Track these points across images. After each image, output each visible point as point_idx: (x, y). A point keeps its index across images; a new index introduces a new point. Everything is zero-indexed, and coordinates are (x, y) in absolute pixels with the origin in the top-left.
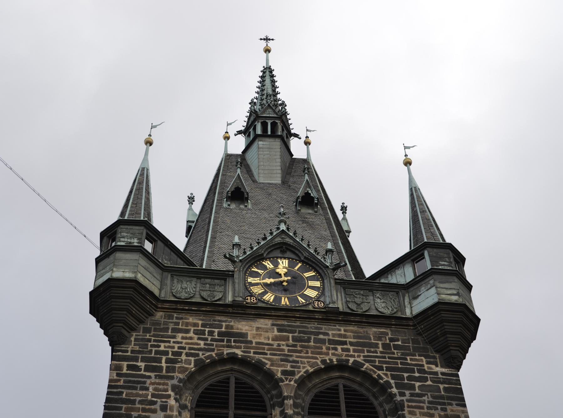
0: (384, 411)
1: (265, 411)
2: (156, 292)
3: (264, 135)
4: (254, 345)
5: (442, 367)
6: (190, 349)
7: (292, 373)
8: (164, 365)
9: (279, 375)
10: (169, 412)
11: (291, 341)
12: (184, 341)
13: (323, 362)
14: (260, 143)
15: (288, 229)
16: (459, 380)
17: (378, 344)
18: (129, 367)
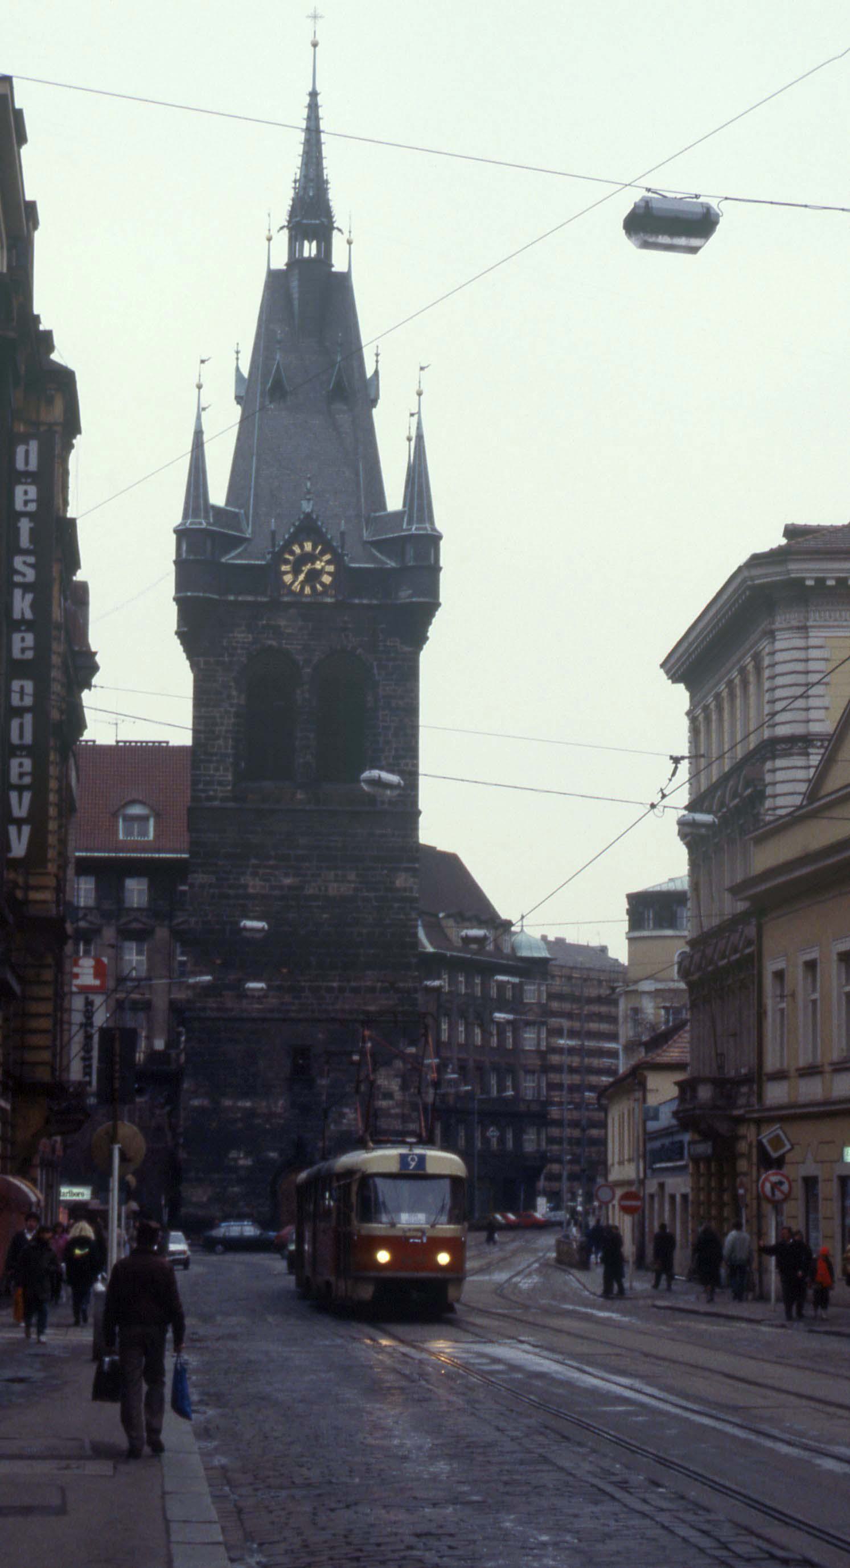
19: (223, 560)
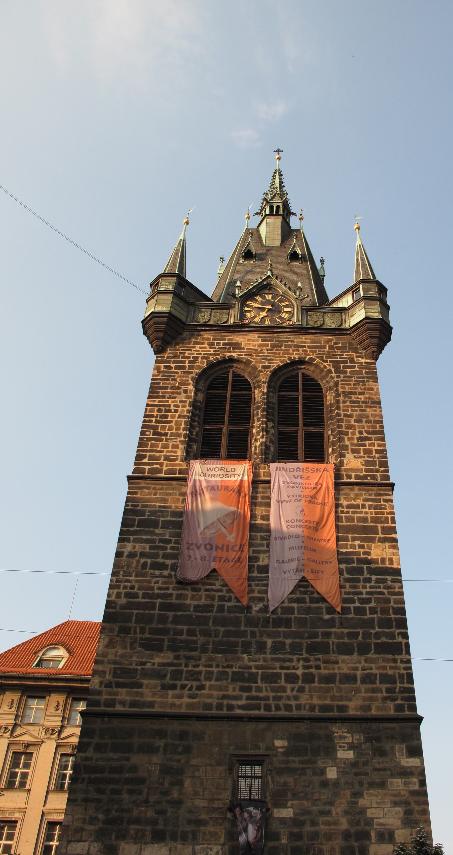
0: (326, 388)
1: (251, 391)
2: (184, 319)
3: (271, 214)
4: (245, 350)
5: (366, 359)
6: (204, 354)
7: (269, 367)
8: (187, 365)
9: (260, 368)
10: (188, 394)
11: (269, 347)
12: (201, 350)
13: (290, 359)
14: (268, 220)
15: (272, 275)
16: (376, 366)
17: (326, 346)
18: (165, 367)
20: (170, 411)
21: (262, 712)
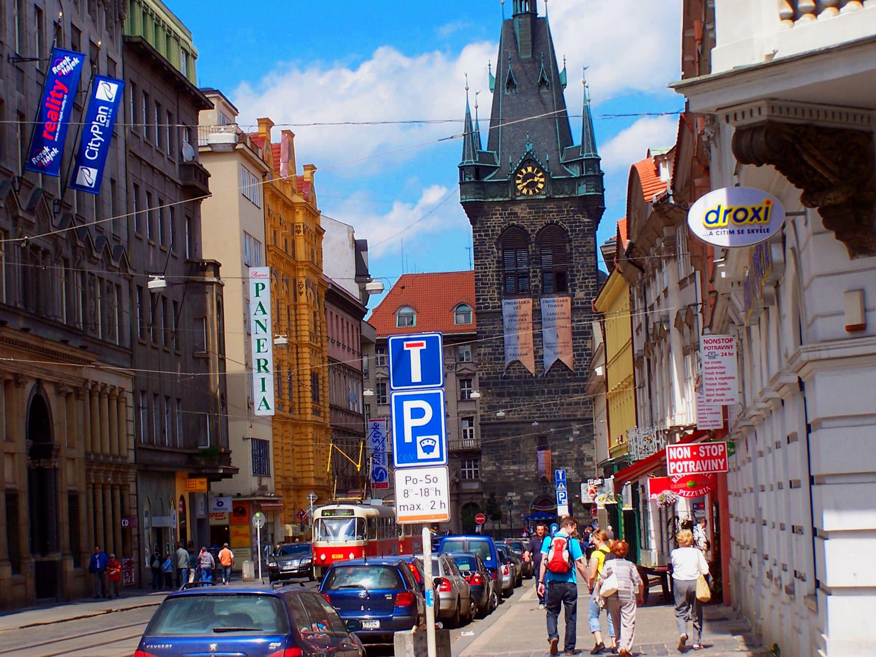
19: (485, 180)
20: (486, 268)
21: (546, 419)
